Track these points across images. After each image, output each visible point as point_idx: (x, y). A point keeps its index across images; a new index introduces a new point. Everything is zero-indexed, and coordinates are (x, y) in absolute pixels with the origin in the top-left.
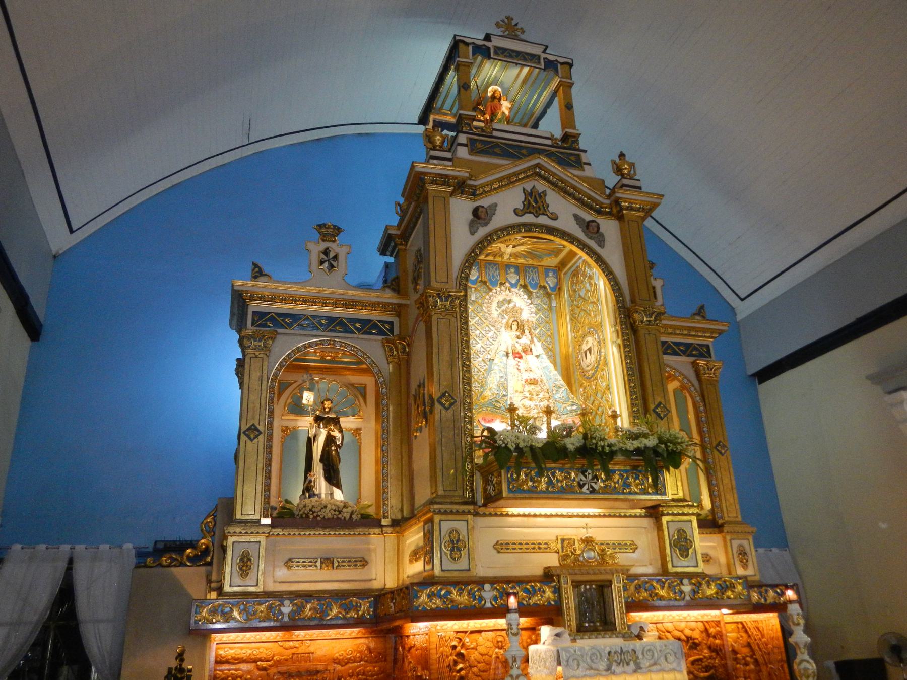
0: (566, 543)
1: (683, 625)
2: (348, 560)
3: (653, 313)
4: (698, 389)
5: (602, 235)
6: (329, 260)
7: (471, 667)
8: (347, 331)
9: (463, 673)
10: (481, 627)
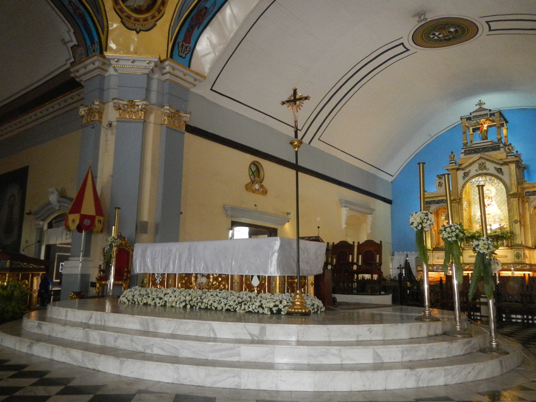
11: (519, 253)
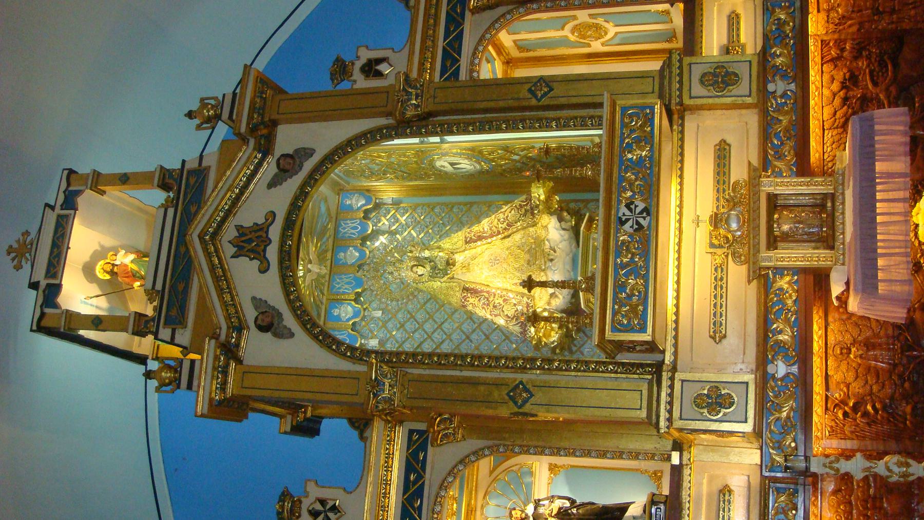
0: (716, 242)
1: (826, 92)
2: (721, 512)
3: (407, 92)
4: (510, 7)
5: (297, 151)
6: (325, 511)
7: (871, 393)
8: (419, 493)
9: (878, 406)
10: (822, 376)
11: (704, 75)
